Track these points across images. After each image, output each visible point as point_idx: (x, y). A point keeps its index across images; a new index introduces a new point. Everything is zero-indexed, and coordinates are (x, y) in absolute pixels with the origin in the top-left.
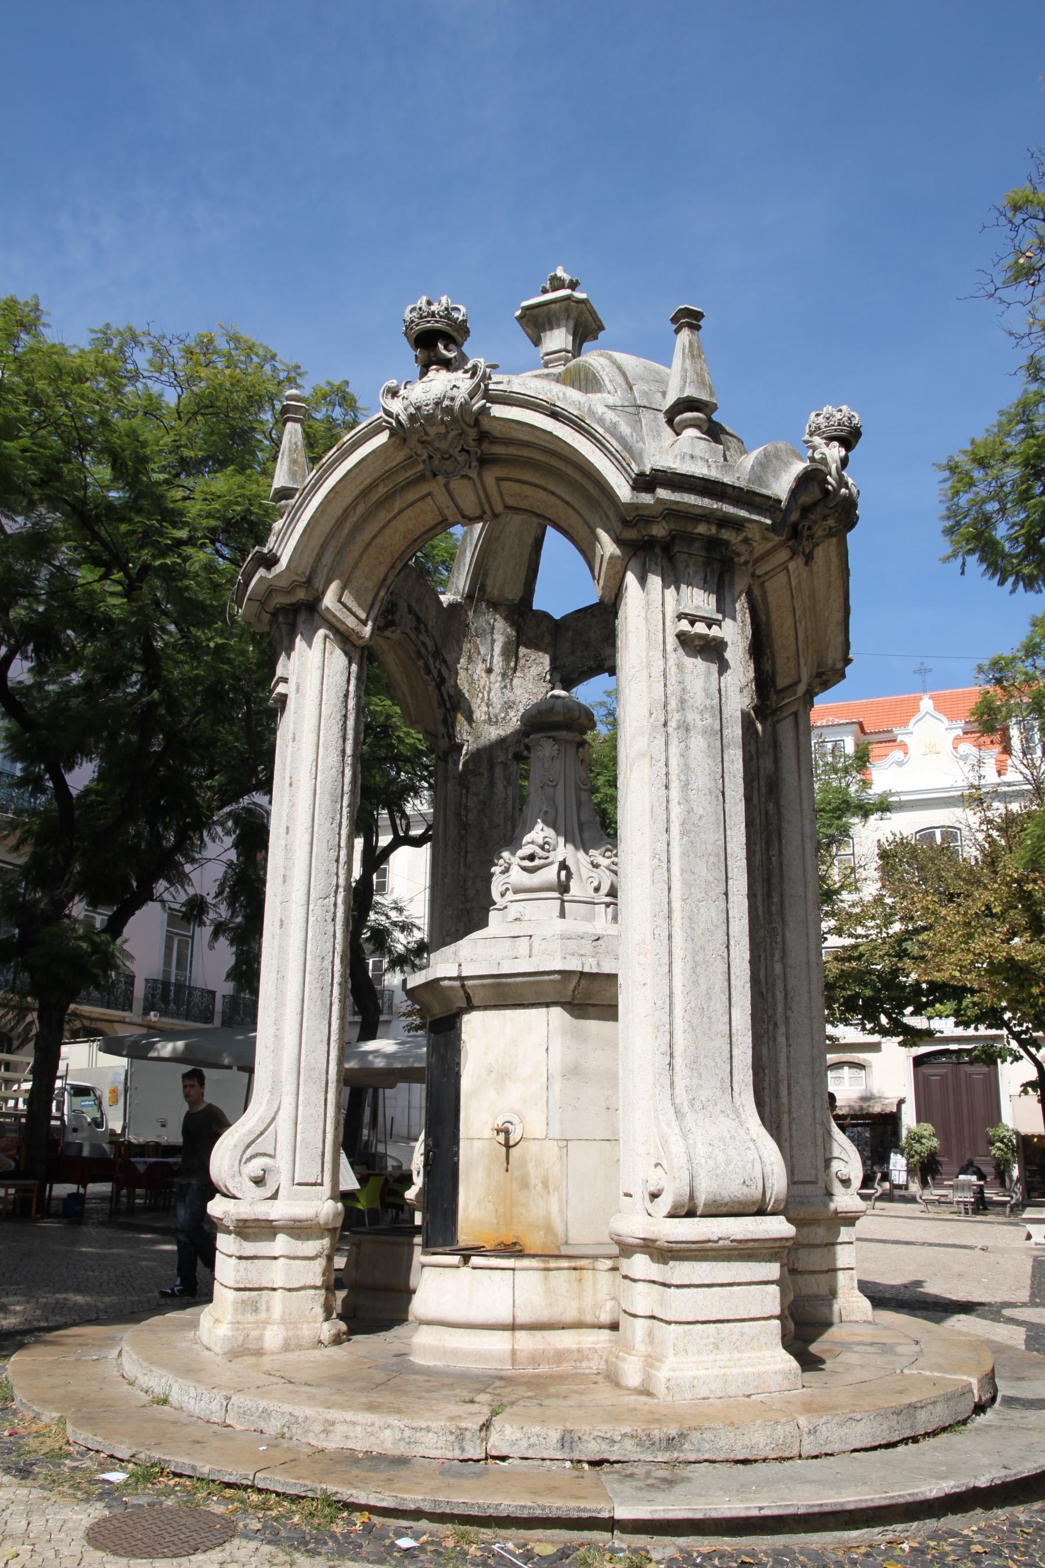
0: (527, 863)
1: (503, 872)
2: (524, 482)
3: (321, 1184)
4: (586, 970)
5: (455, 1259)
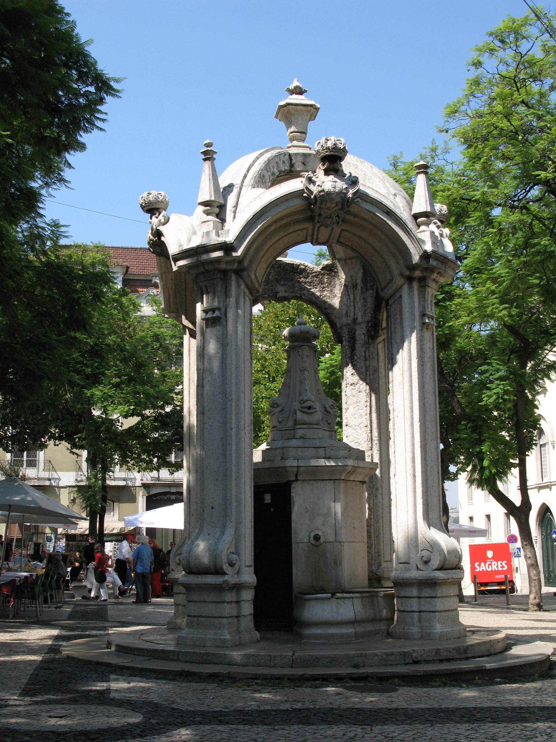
0: (306, 410)
1: (281, 411)
2: (355, 235)
3: (251, 566)
4: (355, 465)
5: (330, 595)
